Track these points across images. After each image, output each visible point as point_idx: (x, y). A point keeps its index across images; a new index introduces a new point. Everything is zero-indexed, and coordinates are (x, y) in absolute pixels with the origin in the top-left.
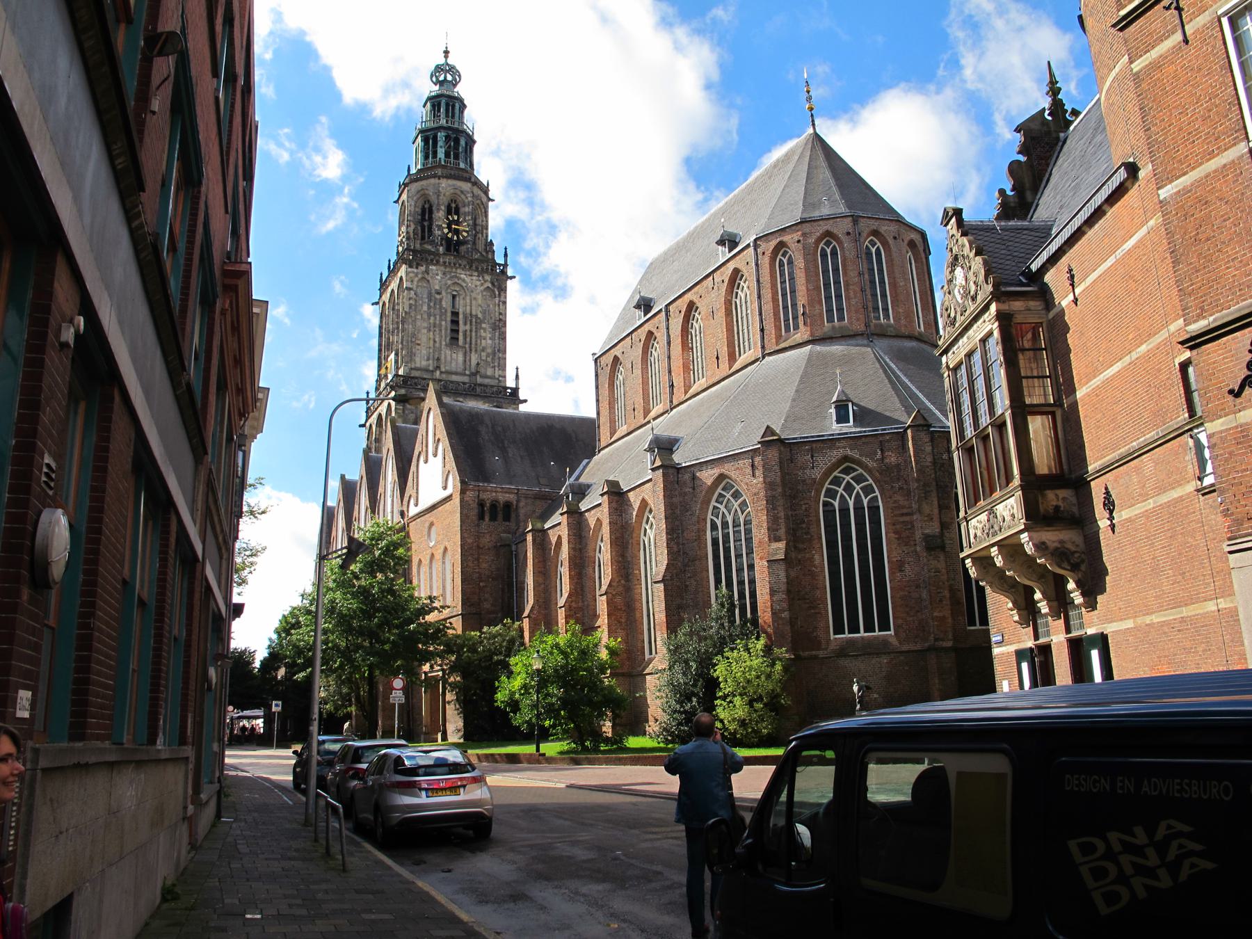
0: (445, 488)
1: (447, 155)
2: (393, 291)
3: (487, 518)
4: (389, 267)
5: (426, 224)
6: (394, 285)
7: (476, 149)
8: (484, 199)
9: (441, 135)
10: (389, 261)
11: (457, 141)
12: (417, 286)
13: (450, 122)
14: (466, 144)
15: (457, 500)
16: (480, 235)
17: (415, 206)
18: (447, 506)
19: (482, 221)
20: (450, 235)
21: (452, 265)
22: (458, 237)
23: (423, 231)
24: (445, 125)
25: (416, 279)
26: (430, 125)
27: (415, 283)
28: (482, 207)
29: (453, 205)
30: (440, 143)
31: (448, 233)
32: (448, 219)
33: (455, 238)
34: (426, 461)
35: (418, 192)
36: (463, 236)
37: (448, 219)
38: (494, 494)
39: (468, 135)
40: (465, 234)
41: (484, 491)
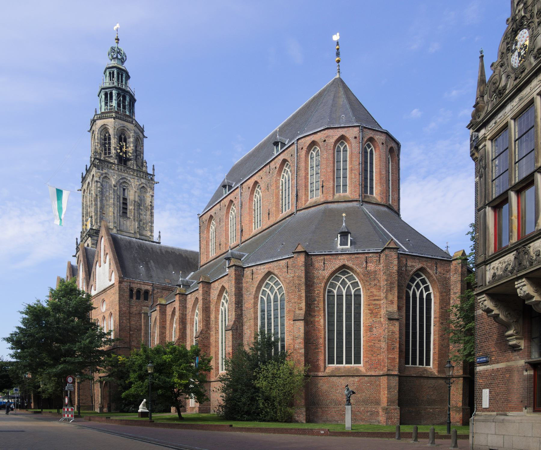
0: (110, 280)
1: (119, 105)
2: (89, 183)
3: (135, 298)
4: (86, 169)
5: (107, 146)
6: (89, 179)
7: (136, 104)
8: (141, 136)
9: (114, 92)
10: (86, 166)
11: (124, 98)
12: (103, 181)
13: (120, 85)
14: (130, 100)
15: (117, 287)
16: (139, 157)
17: (101, 135)
18: (112, 290)
19: (140, 149)
20: (121, 154)
21: (123, 171)
22: (126, 156)
23: (105, 150)
24: (117, 86)
25: (102, 177)
26: (107, 85)
27: (101, 179)
28: (140, 140)
29: (123, 136)
30: (114, 97)
31: (120, 152)
32: (120, 144)
33: (124, 156)
34: (100, 266)
35: (102, 126)
36: (129, 155)
37: (120, 144)
38: (139, 285)
39: (131, 95)
40: (130, 155)
41: (133, 283)
